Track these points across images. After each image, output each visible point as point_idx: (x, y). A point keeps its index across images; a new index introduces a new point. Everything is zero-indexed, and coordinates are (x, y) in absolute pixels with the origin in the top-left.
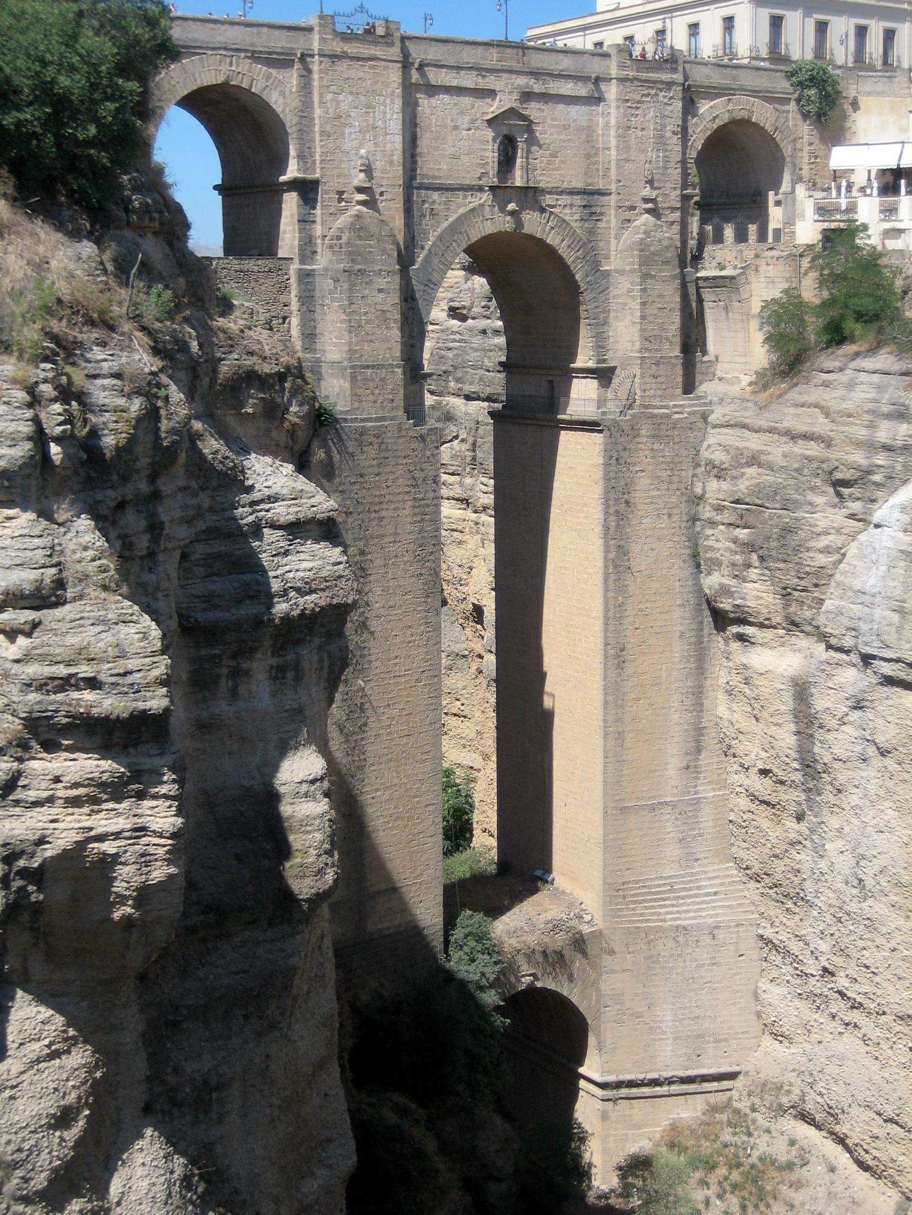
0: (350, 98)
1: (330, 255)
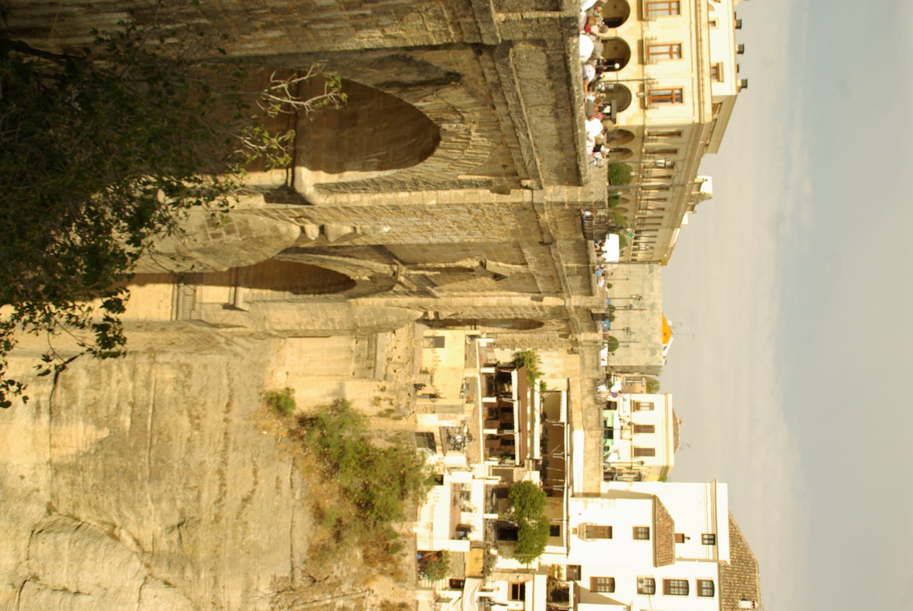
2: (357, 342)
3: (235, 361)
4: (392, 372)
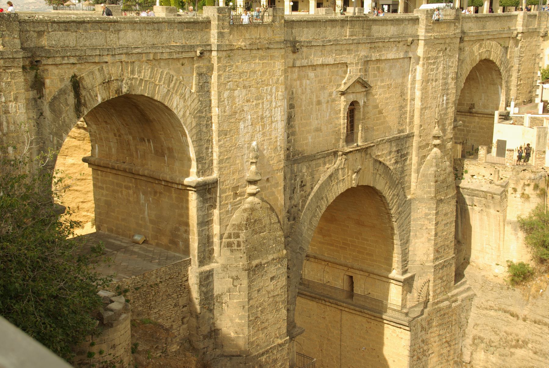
0: (244, 92)
1: (228, 253)
2: (476, 206)
3: (476, 301)
4: (502, 181)
